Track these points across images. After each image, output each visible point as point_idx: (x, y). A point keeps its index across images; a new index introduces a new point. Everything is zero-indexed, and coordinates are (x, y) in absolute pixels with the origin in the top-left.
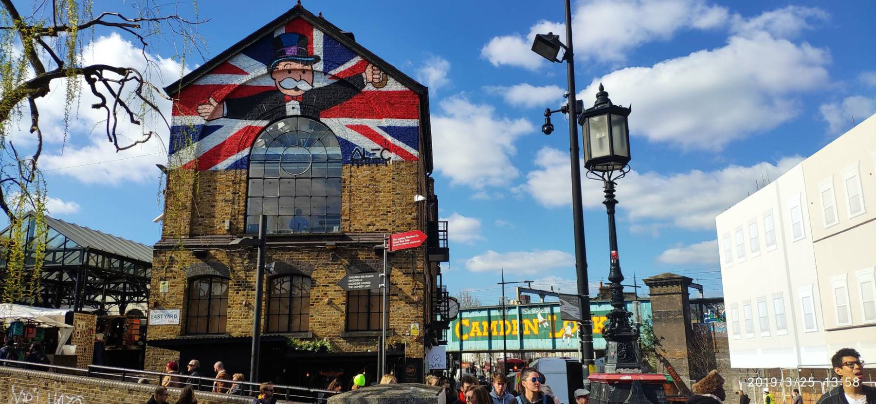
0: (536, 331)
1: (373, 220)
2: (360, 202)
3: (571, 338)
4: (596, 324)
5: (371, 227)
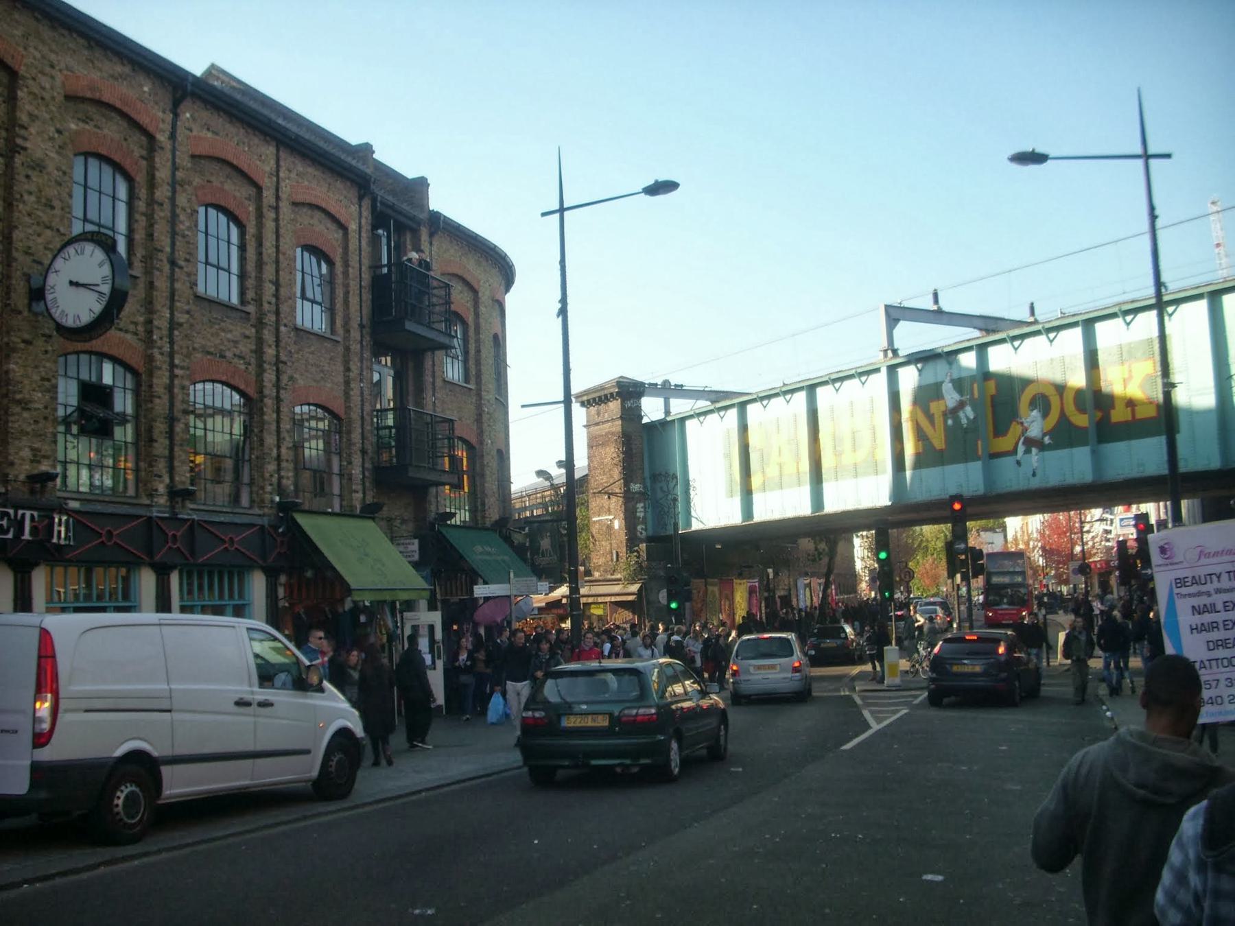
3: (1042, 447)
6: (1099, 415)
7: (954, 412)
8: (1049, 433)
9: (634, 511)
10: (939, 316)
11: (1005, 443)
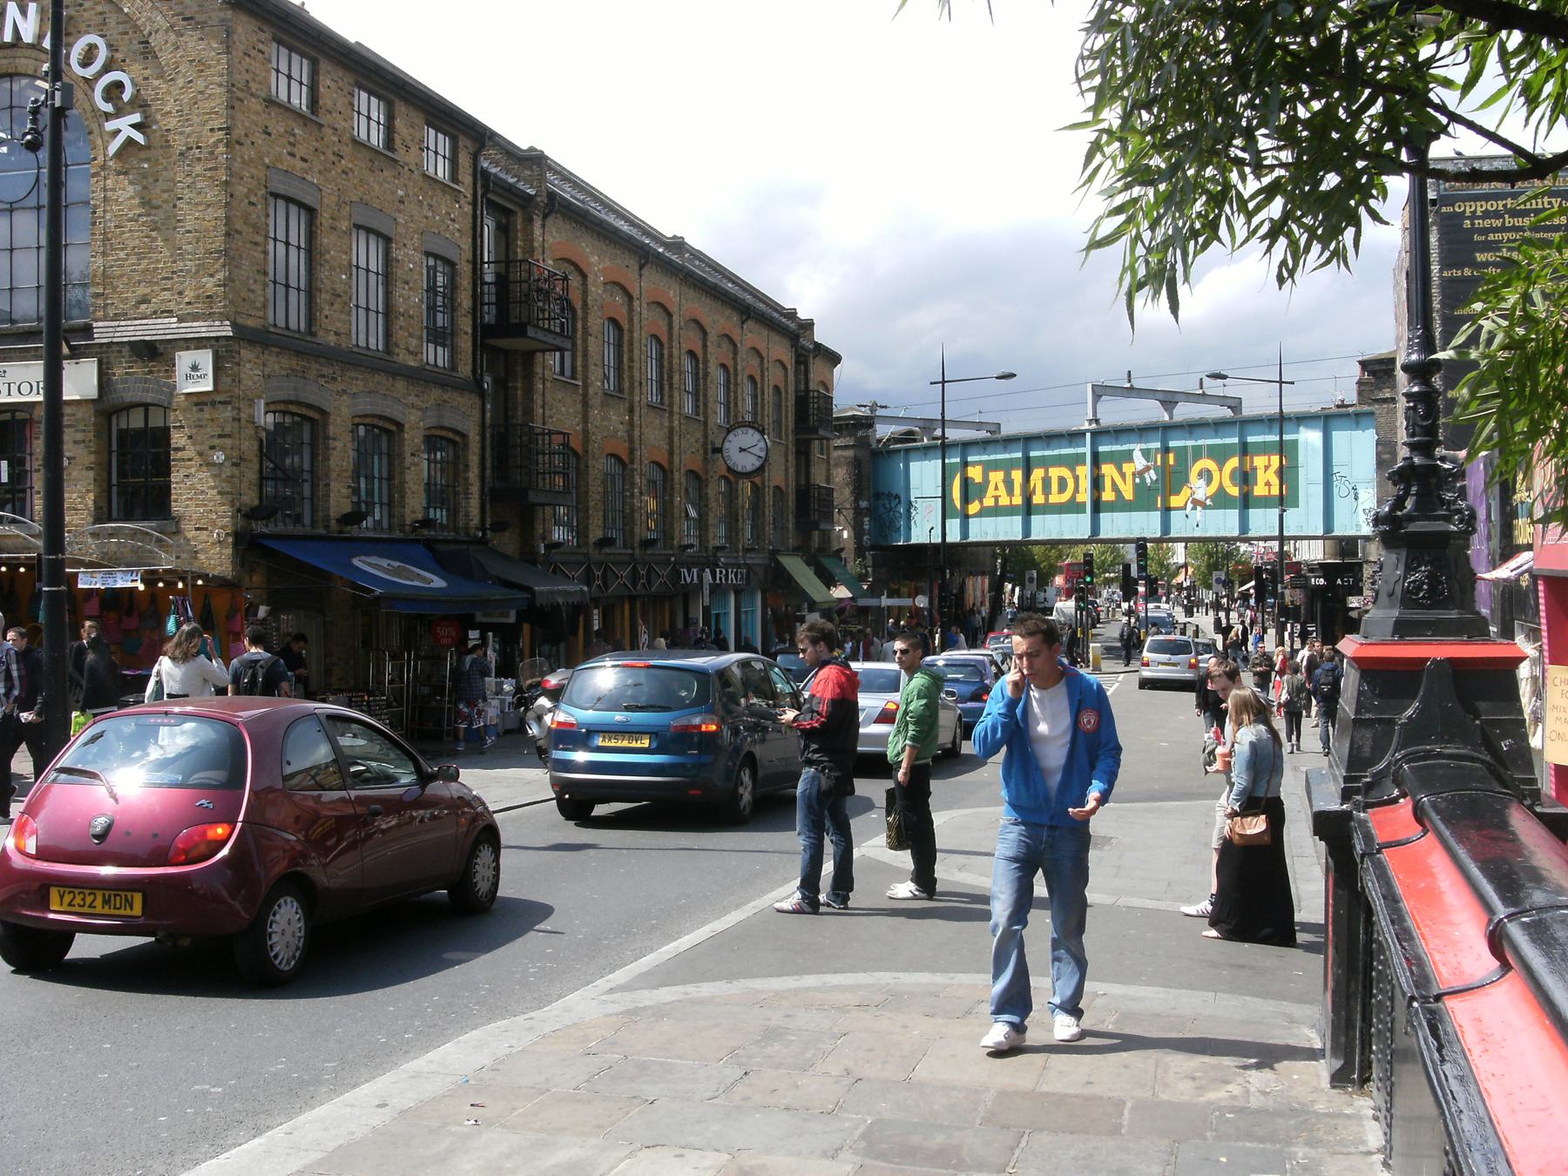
0: (1128, 495)
1: (148, 290)
2: (122, 255)
3: (1205, 507)
4: (1260, 472)
5: (143, 306)
7: (1141, 474)
8: (1212, 497)
9: (862, 524)
10: (1132, 392)
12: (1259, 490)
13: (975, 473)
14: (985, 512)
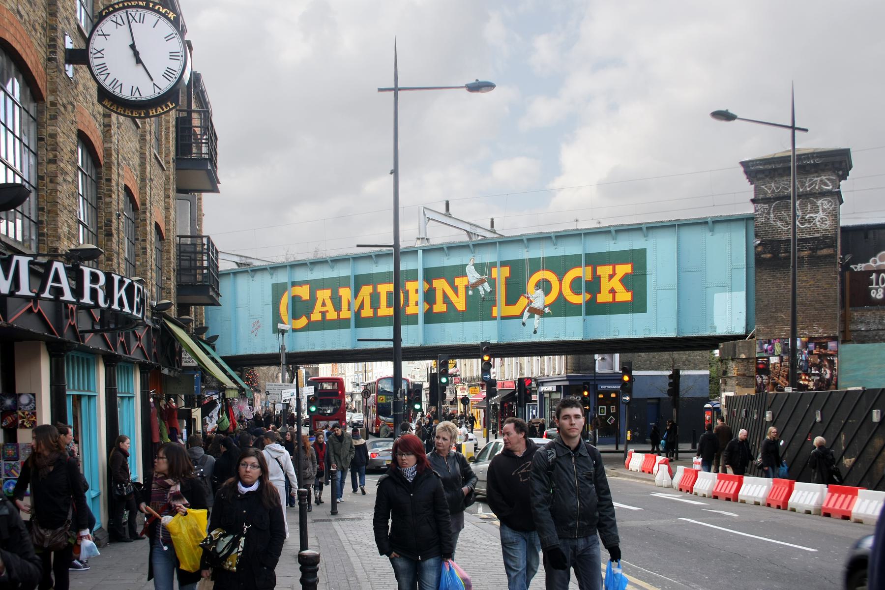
3: (542, 314)
6: (588, 296)
7: (474, 286)
8: (549, 306)
11: (514, 310)
12: (604, 297)
13: (303, 292)
14: (311, 326)
